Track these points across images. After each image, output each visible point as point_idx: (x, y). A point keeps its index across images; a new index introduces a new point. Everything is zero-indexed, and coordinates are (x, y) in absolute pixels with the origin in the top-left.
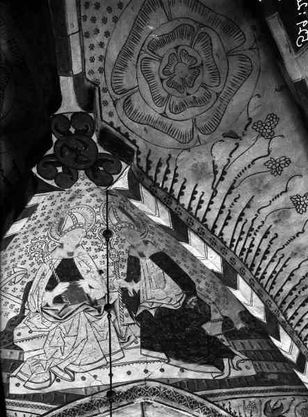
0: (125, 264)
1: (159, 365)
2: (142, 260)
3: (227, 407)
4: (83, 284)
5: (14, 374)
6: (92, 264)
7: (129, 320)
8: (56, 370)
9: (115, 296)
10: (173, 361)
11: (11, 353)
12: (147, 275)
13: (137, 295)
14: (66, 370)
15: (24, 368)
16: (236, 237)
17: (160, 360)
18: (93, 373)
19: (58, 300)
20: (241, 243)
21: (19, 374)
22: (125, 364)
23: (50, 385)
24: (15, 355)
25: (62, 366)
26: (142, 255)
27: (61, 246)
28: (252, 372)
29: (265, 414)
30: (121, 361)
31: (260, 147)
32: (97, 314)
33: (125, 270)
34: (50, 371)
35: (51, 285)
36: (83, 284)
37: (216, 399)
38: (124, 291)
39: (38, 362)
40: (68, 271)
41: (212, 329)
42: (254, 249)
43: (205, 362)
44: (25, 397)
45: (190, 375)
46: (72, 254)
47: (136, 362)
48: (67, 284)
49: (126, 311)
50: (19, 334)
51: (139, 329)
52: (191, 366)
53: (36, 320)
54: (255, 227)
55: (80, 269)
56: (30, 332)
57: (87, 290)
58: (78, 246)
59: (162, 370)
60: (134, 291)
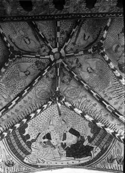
0: (63, 136)
1: (72, 161)
2: (67, 133)
3: (96, 167)
4: (52, 141)
5: (27, 156)
6: (54, 137)
7: (63, 150)
8: (39, 159)
9: (60, 145)
10: (76, 159)
11: (29, 149)
12: (68, 137)
13: (65, 144)
14: (42, 160)
15: (30, 156)
16: (85, 111)
17: (72, 160)
18: (50, 162)
19: (45, 142)
20: (86, 112)
21: (28, 157)
22: (61, 161)
23: (36, 163)
24: (29, 151)
25: (41, 159)
26: (67, 132)
27: (49, 129)
28: (100, 150)
29: (108, 163)
30: (61, 160)
31: (85, 99)
32: (54, 148)
33: (62, 138)
34: (37, 159)
35: (44, 138)
36: (52, 141)
37: (92, 166)
38: (62, 143)
39: (35, 156)
40: (48, 136)
41: (86, 143)
42: (89, 113)
43: (86, 156)
44: (28, 164)
45: (82, 162)
46: (50, 132)
47: (65, 161)
48: (48, 140)
49: (62, 148)
50: (33, 145)
51: (66, 152)
52: (82, 159)
53: (38, 144)
54: (88, 109)
55: (51, 137)
56: (36, 147)
57: (52, 143)
58: (52, 131)
59: (73, 162)
60: (64, 143)
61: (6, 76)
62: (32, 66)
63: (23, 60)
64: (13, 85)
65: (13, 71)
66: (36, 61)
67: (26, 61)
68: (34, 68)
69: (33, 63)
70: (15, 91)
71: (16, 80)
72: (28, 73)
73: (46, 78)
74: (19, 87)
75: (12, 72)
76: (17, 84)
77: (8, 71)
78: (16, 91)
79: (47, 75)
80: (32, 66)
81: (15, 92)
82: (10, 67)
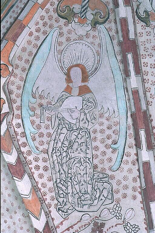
61: (50, 184)
62: (63, 39)
63: (22, 64)
64: (92, 179)
65: (45, 139)
66: (56, 10)
67: (34, 51)
68: (73, 36)
69: (55, 25)
70: (115, 187)
71: (82, 155)
72: (76, 74)
73: (148, 29)
74: (110, 160)
75: (45, 146)
76: (97, 156)
77: (34, 164)
78: (119, 183)
79: (139, 18)
80: (63, 39)
81: (122, 191)
82: (25, 145)
